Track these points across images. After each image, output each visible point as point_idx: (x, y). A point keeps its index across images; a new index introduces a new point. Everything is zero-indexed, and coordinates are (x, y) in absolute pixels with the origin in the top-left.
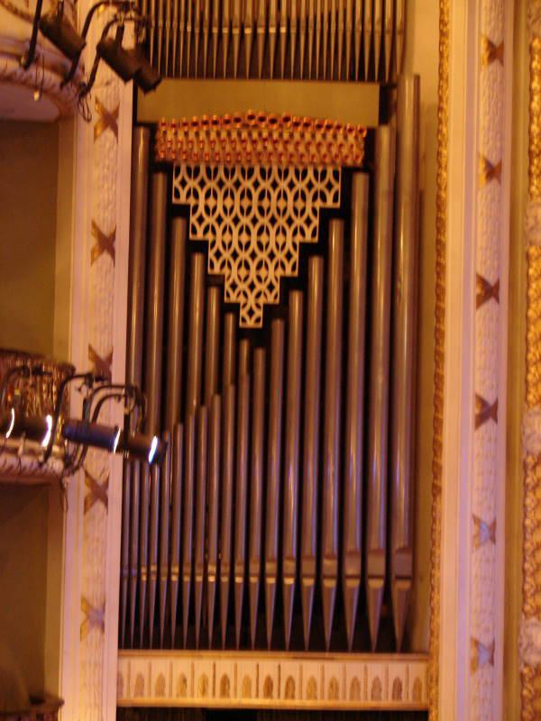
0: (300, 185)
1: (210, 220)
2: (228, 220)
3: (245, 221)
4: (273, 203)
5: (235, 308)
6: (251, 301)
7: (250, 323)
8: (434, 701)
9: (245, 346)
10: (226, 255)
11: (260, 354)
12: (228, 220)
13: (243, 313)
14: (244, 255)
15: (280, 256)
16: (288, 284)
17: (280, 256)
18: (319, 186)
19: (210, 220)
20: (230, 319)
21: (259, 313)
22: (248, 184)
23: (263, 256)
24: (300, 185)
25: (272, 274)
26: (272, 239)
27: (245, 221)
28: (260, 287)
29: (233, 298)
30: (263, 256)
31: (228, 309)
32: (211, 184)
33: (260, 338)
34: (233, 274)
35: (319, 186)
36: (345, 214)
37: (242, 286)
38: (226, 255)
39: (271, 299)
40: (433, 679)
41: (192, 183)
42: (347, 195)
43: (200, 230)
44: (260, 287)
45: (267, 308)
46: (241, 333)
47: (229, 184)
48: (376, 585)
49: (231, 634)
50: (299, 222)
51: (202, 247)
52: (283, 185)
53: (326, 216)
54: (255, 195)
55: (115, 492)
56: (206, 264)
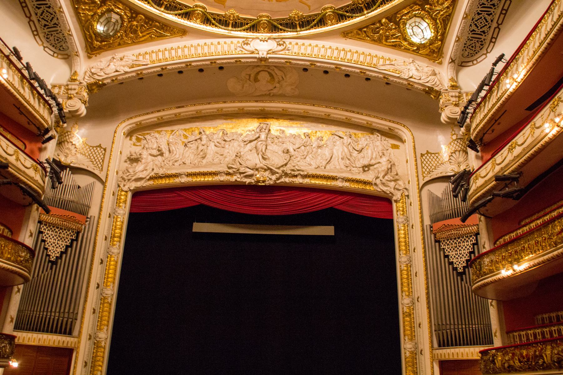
0: (68, 233)
1: (47, 236)
2: (51, 237)
3: (55, 238)
4: (62, 235)
5: (49, 256)
6: (53, 255)
7: (52, 259)
8: (78, 347)
9: (50, 264)
10: (50, 244)
11: (54, 266)
12: (51, 237)
13: (51, 257)
14: (54, 245)
15: (61, 246)
16: (62, 253)
17: (61, 246)
18: (72, 234)
19: (47, 236)
20: (48, 258)
21: (55, 258)
22: (57, 230)
23: (58, 246)
24: (68, 233)
25: (59, 250)
26: (60, 242)
27: (55, 238)
28: (56, 252)
29: (50, 253)
30: (58, 246)
31: (48, 255)
32: (49, 228)
33: (54, 263)
34: (51, 248)
35: (72, 234)
36: (77, 240)
37: (52, 251)
38: (50, 244)
39: (58, 255)
40: (79, 342)
41: (45, 227)
42: (77, 237)
43: (45, 237)
44: (56, 252)
45: (57, 257)
46: (50, 261)
47: (53, 229)
48: (65, 319)
49: (33, 328)
50: (67, 240)
51: (44, 241)
52: (65, 232)
53: (72, 240)
54: (58, 232)
55: (21, 291)
56: (45, 245)
